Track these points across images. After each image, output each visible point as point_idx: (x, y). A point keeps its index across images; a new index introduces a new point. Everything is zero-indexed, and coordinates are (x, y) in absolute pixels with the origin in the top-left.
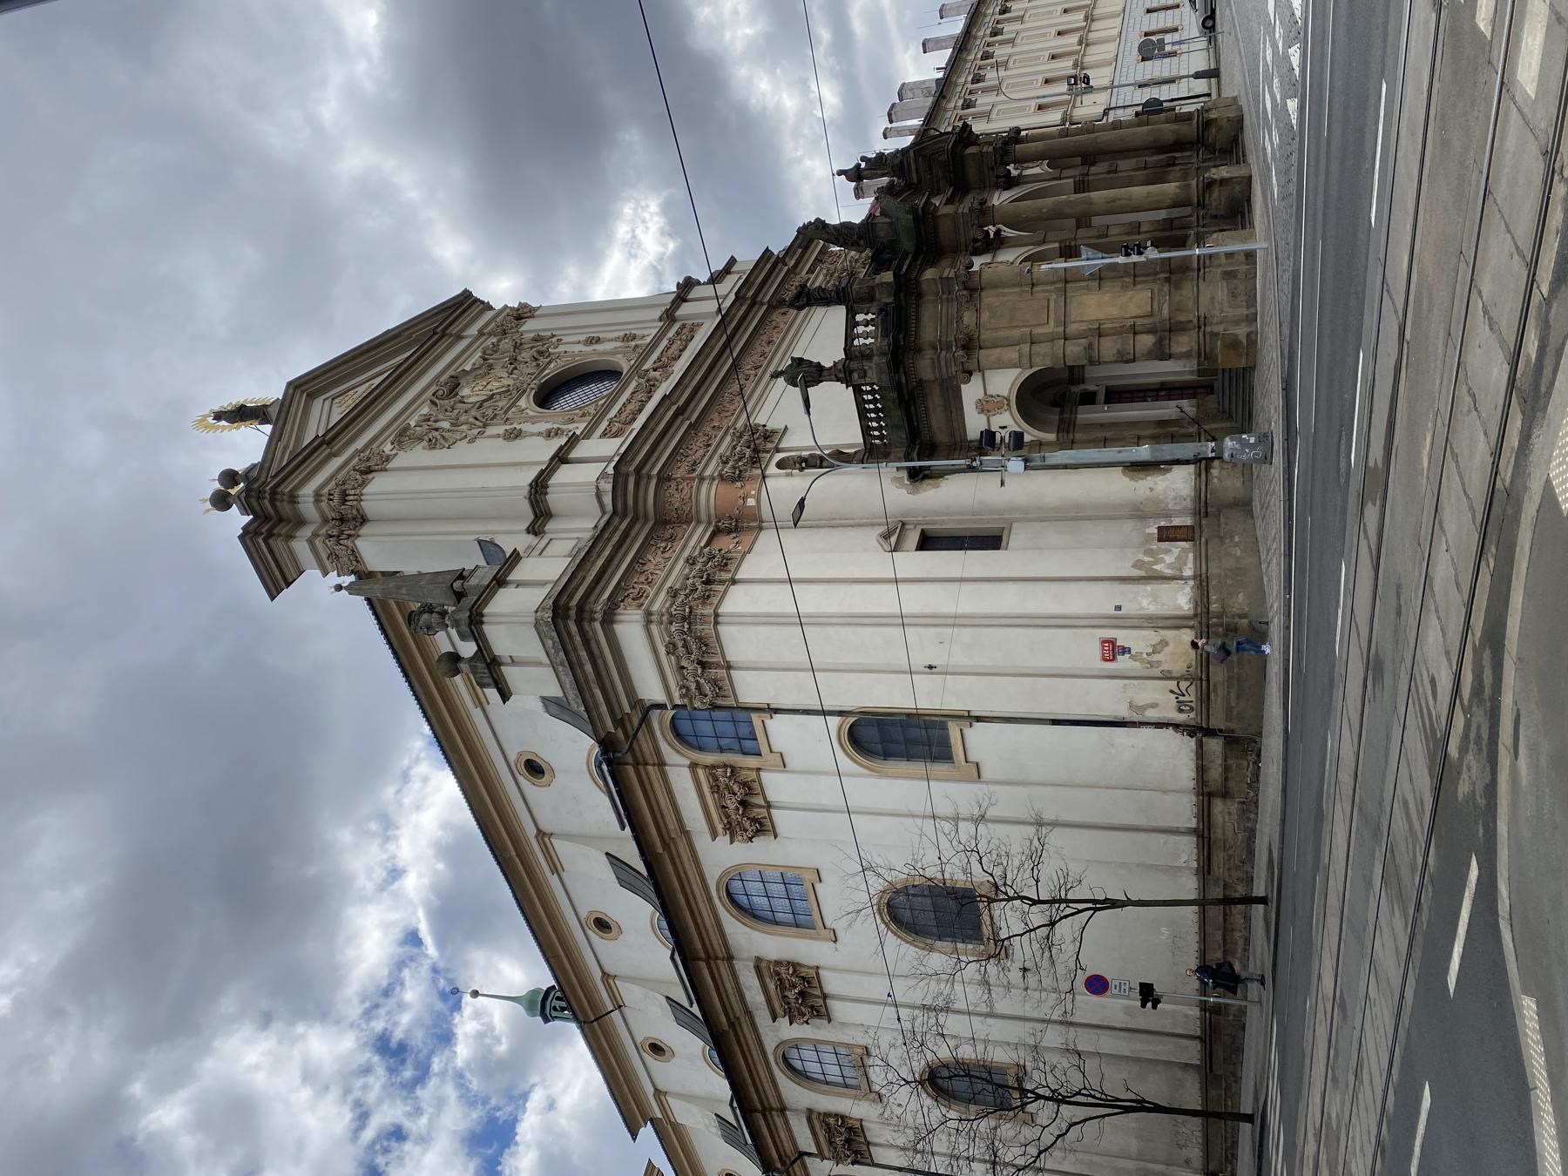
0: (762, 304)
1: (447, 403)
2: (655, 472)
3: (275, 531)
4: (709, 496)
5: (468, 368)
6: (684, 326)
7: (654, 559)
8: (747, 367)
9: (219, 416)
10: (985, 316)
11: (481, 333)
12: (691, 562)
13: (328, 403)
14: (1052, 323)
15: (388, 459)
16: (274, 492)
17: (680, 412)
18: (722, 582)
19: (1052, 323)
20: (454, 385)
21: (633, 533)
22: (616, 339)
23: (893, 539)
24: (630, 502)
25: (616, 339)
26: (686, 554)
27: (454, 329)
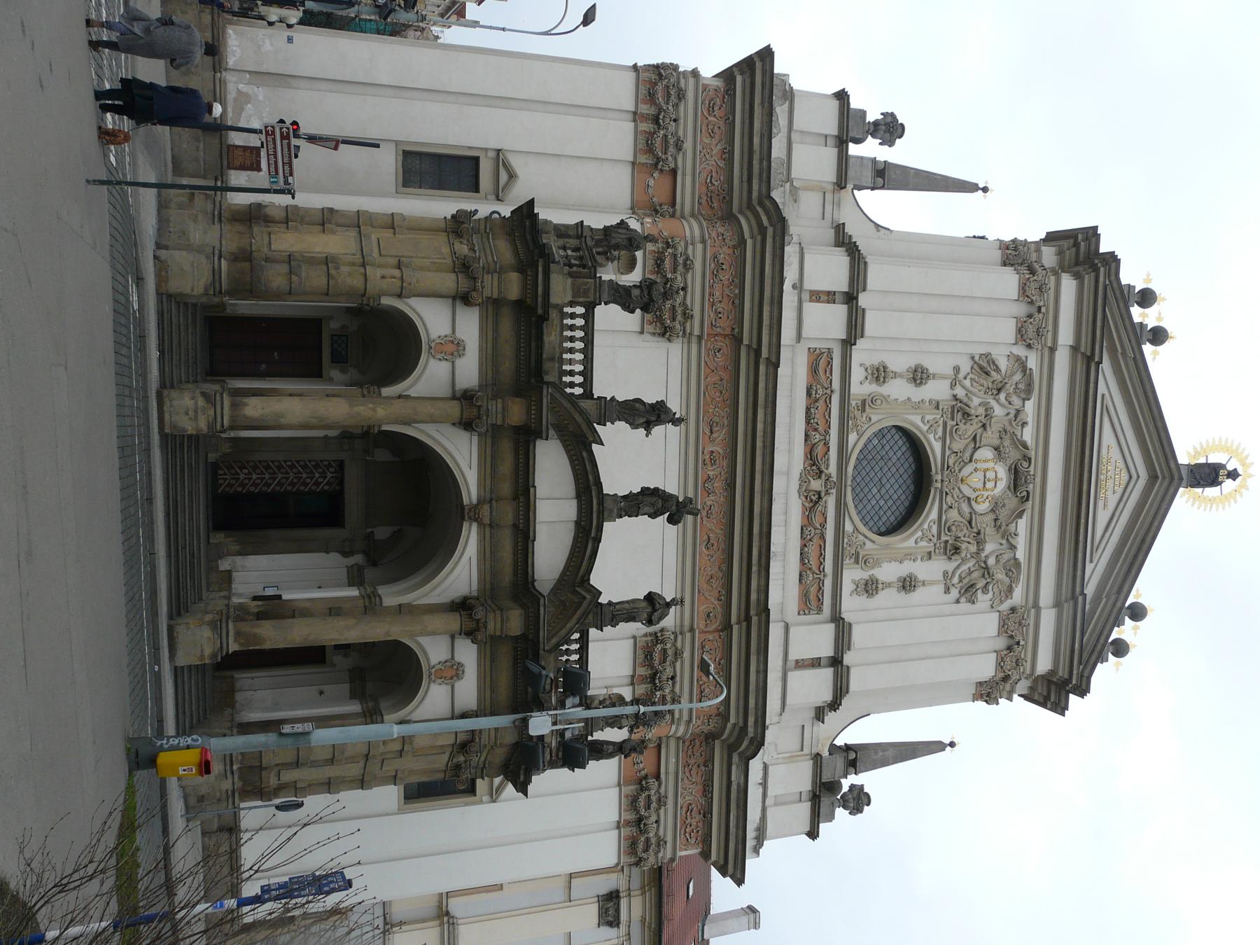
0: (739, 623)
1: (1014, 455)
2: (749, 242)
3: (1074, 250)
4: (692, 229)
5: (1022, 525)
6: (820, 610)
7: (714, 159)
8: (718, 485)
9: (1233, 475)
10: (446, 250)
11: (1036, 606)
12: (679, 147)
13: (1135, 476)
14: (374, 238)
15: (1021, 332)
16: (1096, 270)
17: (758, 352)
18: (644, 118)
19: (374, 238)
20: (1017, 478)
21: (745, 184)
22: (889, 585)
23: (504, 176)
24: (759, 209)
25: (888, 585)
26: (688, 145)
27: (1068, 607)
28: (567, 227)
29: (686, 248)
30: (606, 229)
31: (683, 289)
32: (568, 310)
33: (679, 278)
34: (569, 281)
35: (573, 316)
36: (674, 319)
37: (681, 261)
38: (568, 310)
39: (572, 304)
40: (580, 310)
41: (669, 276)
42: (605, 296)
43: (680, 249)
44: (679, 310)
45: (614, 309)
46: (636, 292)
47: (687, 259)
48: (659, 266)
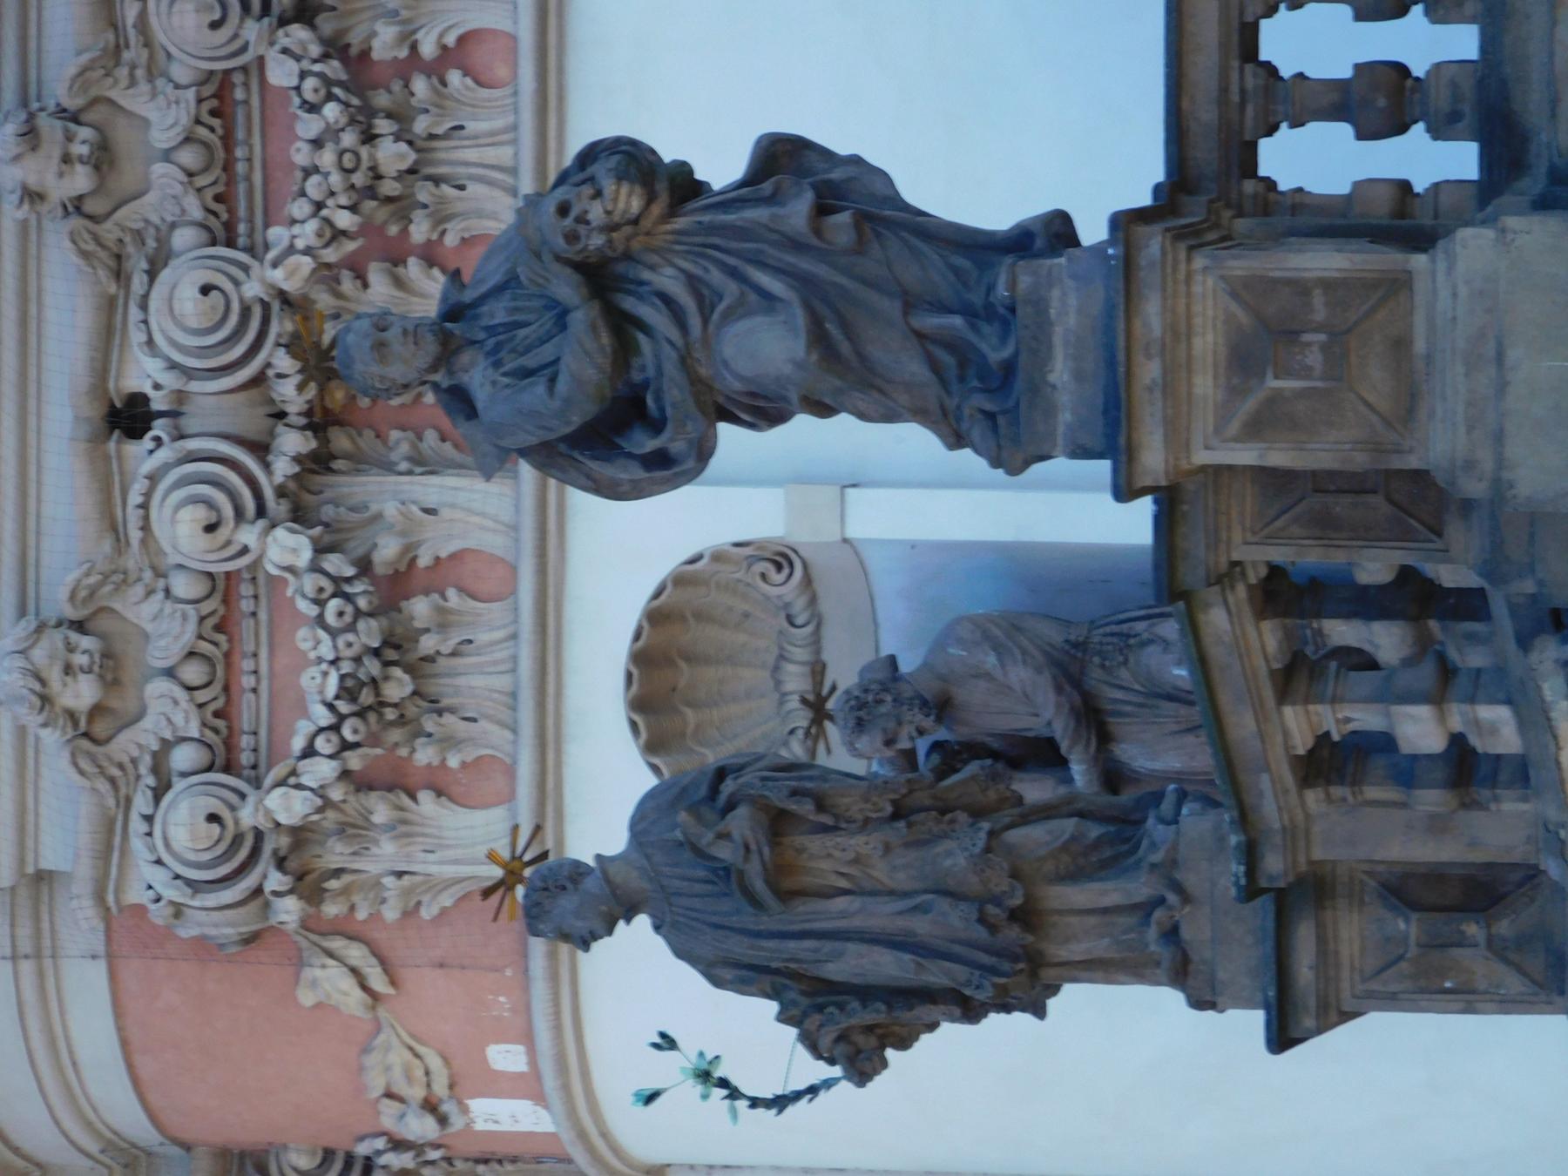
28: (1431, 984)
29: (109, 843)
30: (1022, 981)
31: (129, 418)
32: (1435, 160)
33: (180, 530)
34: (1439, 444)
35: (1381, 102)
36: (220, 98)
37: (166, 711)
38: (1435, 160)
39: (1403, 221)
40: (1310, 159)
41: (287, 547)
42: (1069, 305)
43: (184, 822)
44: (164, 192)
45: (965, 180)
46: (766, 345)
47: (90, 731)
48: (395, 648)
